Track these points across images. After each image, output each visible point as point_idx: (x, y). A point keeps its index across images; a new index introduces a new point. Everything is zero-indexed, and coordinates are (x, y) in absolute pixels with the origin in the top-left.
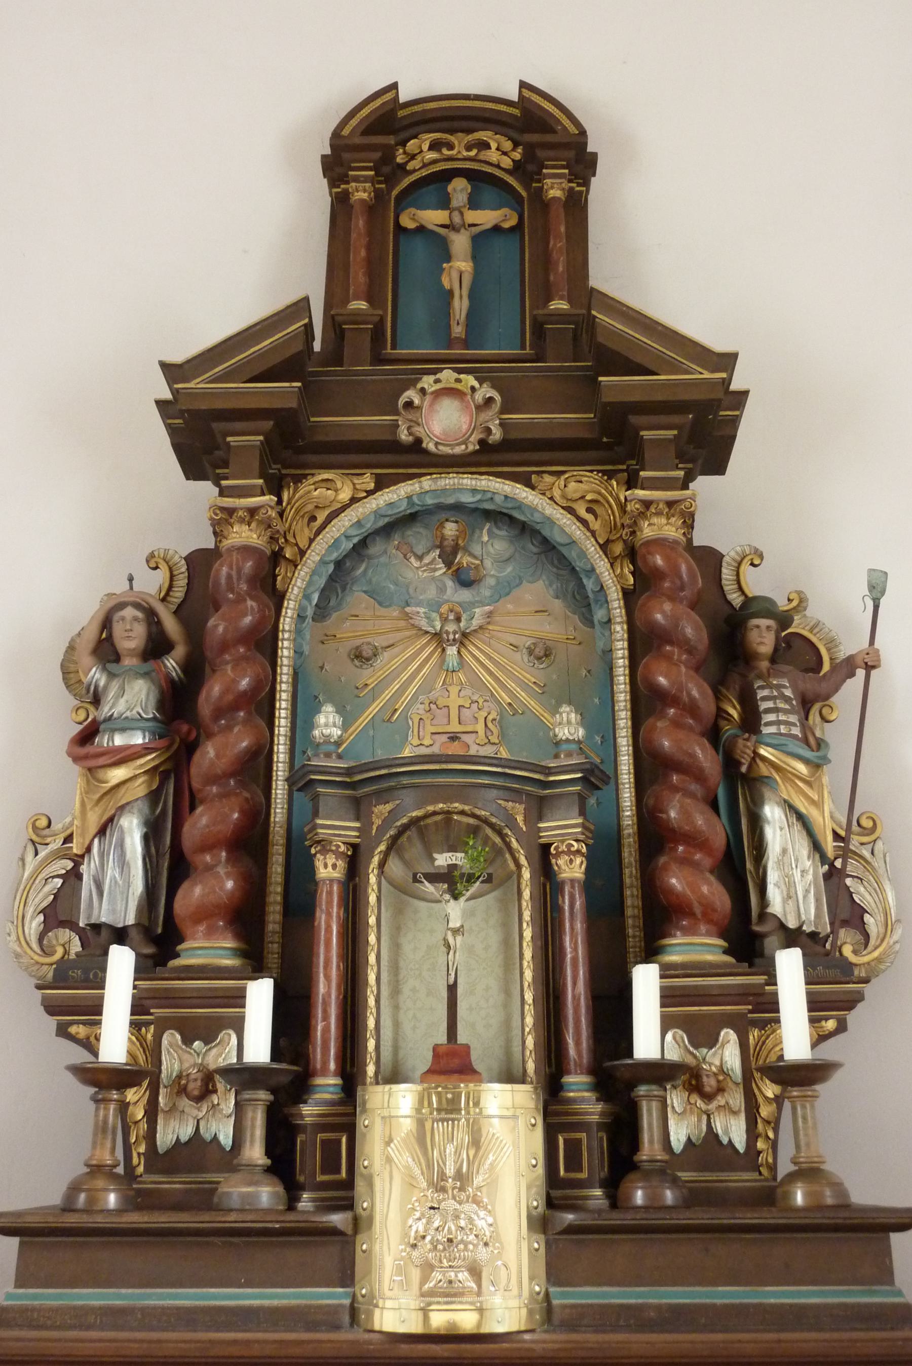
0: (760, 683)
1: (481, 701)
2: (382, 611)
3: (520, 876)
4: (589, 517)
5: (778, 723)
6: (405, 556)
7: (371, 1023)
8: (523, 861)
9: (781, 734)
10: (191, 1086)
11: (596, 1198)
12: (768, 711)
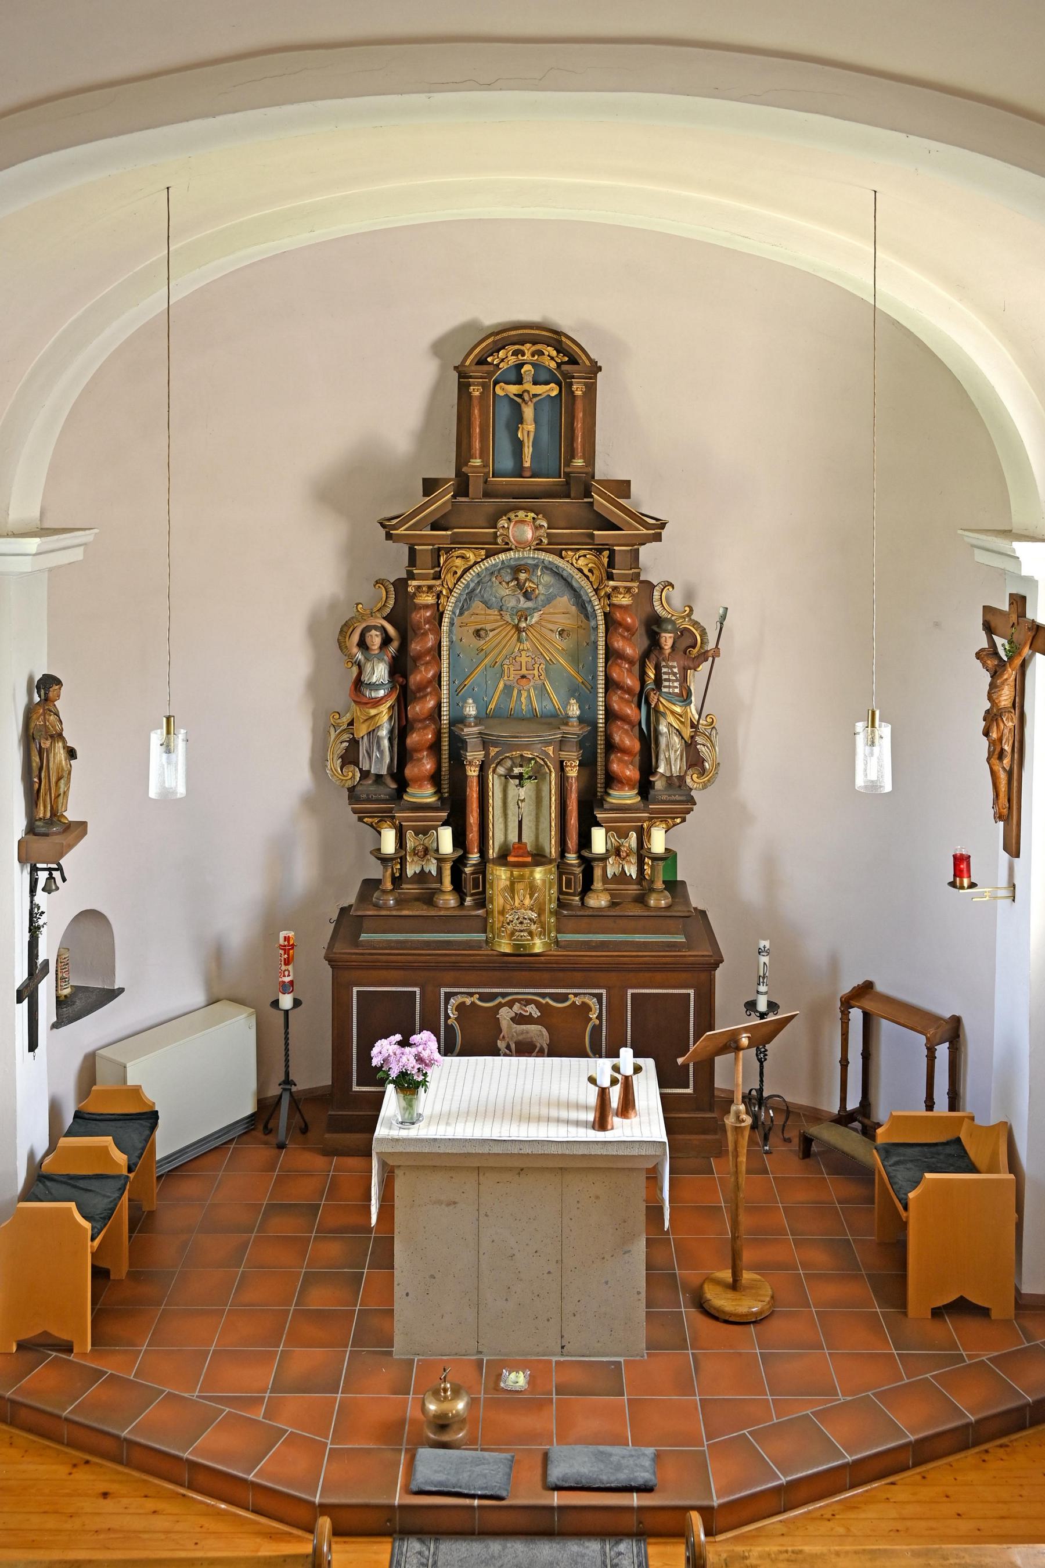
0: (663, 664)
1: (536, 658)
2: (489, 611)
3: (550, 775)
4: (589, 574)
5: (669, 687)
6: (500, 583)
7: (491, 834)
8: (552, 770)
9: (670, 693)
10: (419, 854)
11: (577, 901)
12: (666, 680)
